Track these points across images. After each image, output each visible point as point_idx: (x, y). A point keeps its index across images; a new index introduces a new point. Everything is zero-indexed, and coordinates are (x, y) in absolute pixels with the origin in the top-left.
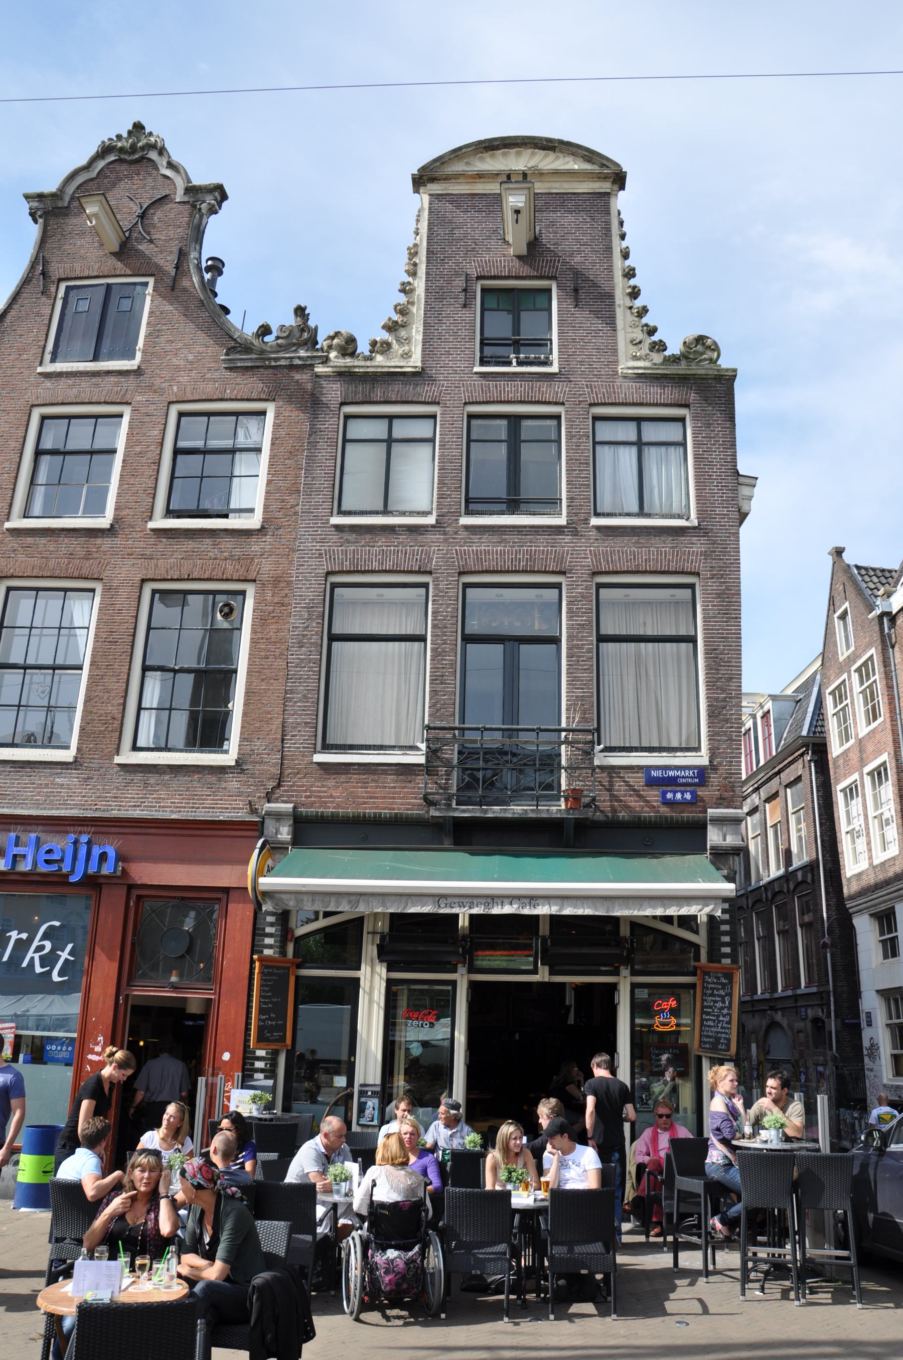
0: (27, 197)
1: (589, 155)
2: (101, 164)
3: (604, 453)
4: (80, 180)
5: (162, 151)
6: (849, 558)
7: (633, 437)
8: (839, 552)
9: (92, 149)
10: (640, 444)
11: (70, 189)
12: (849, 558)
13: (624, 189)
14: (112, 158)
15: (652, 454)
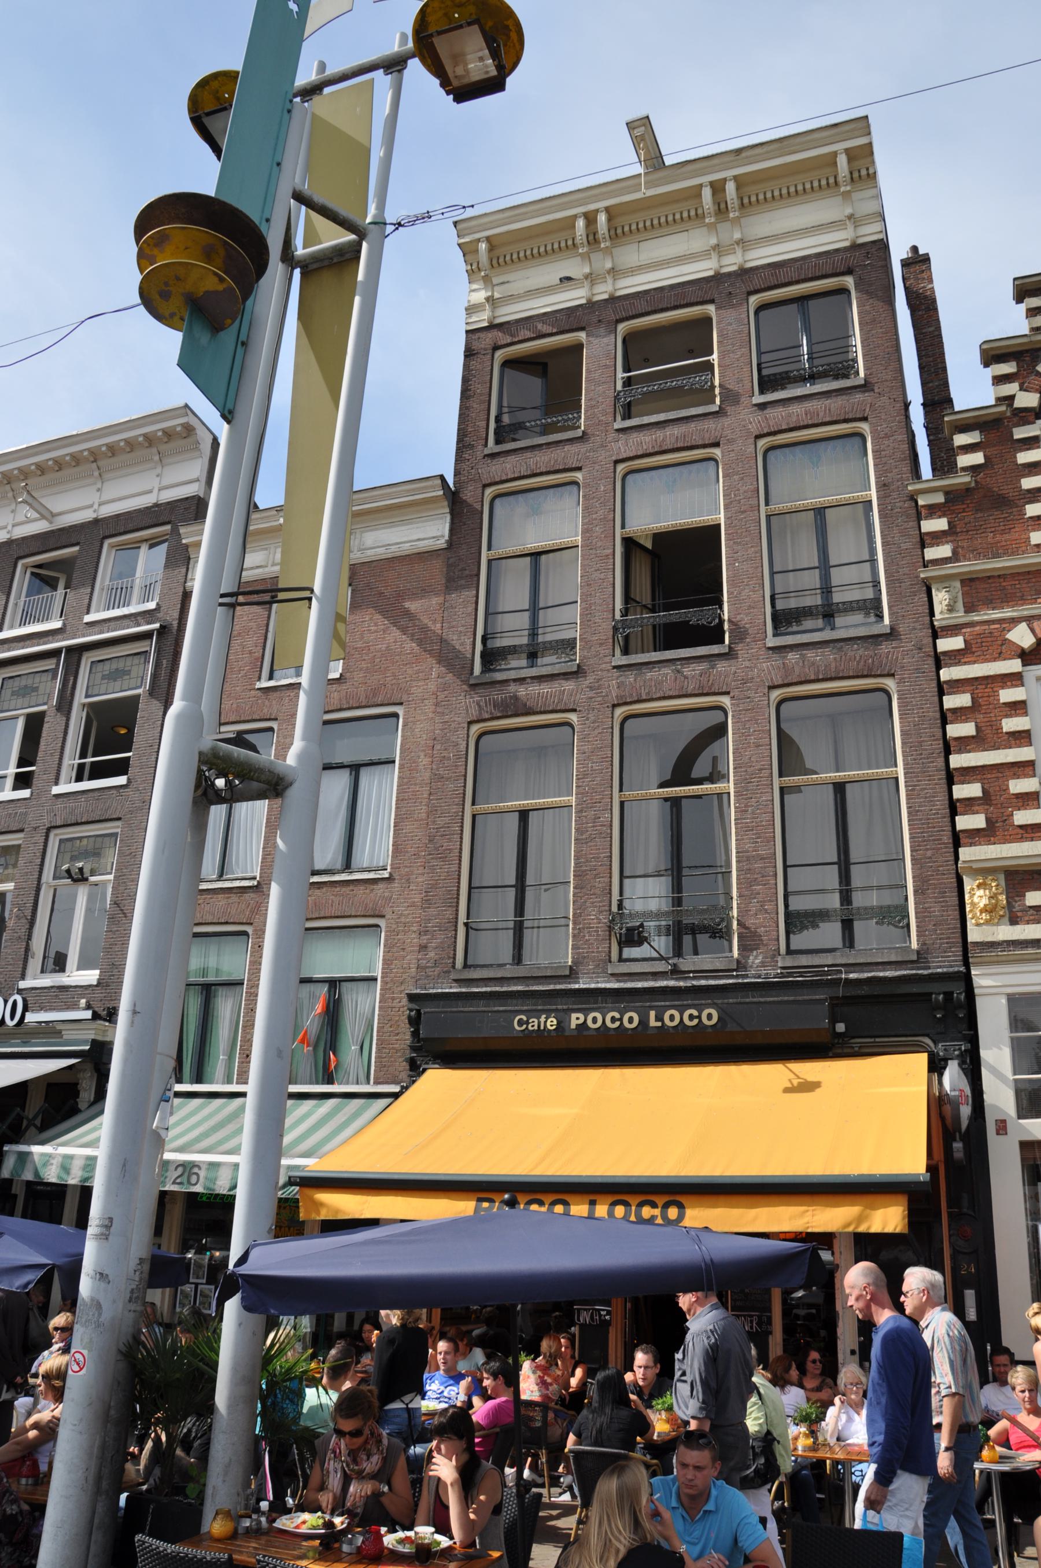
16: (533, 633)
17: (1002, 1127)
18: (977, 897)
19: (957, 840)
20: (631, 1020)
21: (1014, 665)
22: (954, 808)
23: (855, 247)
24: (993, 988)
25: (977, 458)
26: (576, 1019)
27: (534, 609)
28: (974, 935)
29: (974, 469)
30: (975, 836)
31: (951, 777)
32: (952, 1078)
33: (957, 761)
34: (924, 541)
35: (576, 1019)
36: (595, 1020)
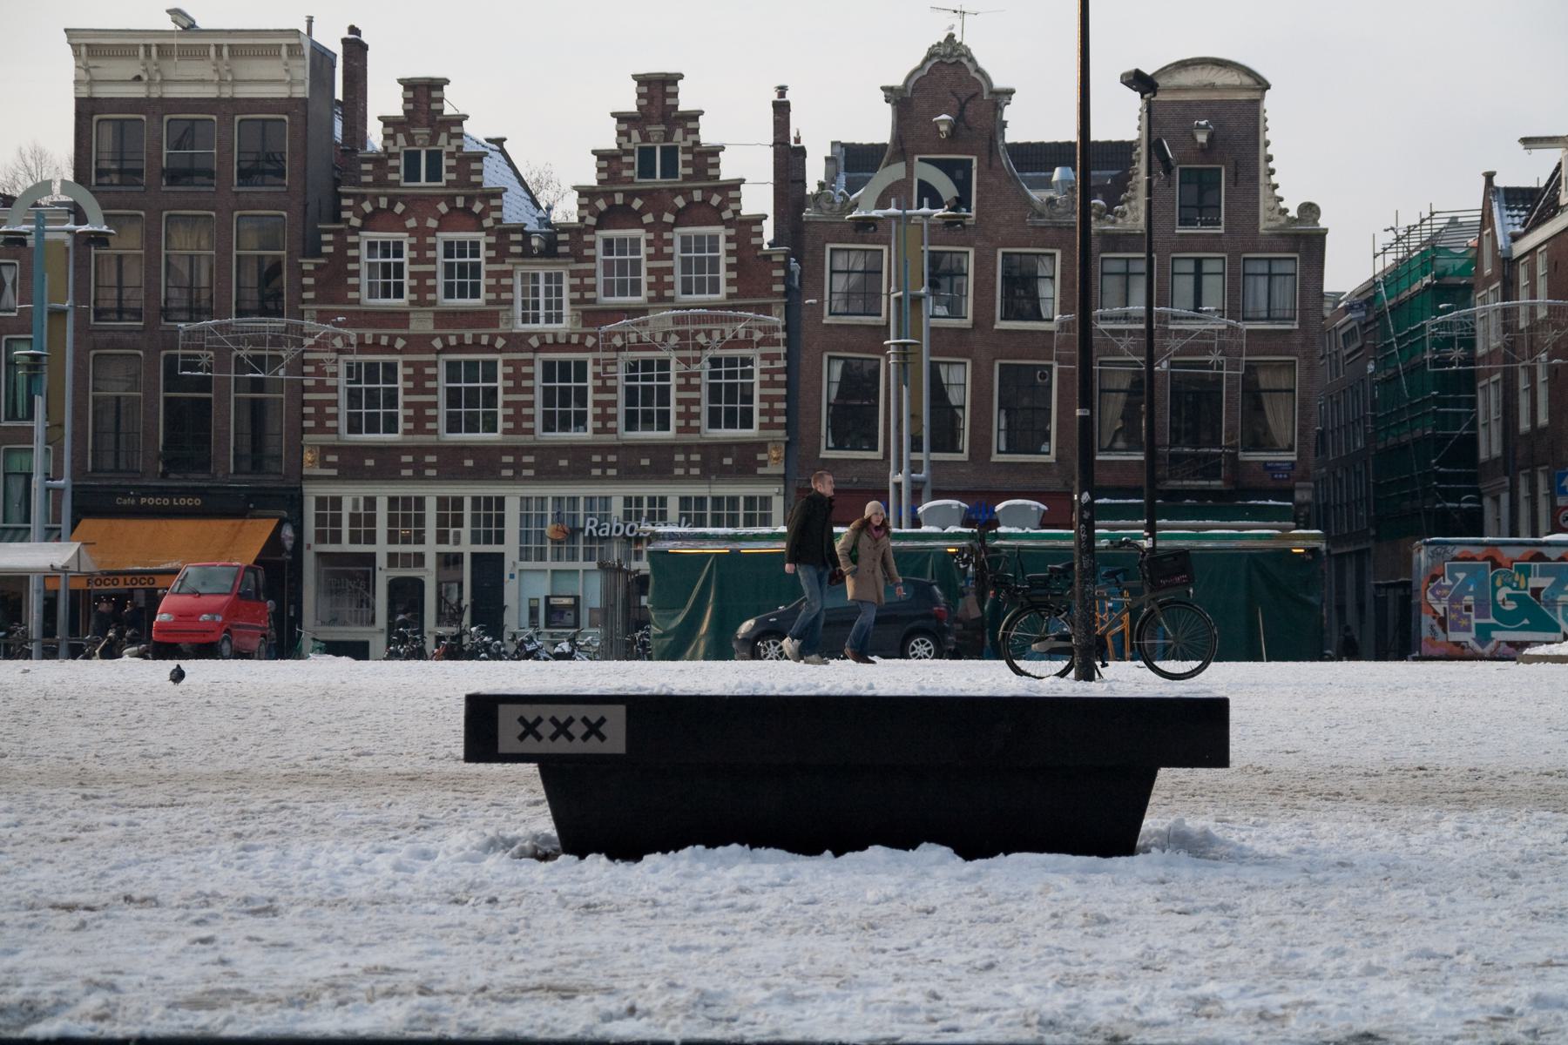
0: (883, 88)
1: (1249, 72)
2: (929, 65)
3: (1251, 280)
4: (917, 77)
5: (972, 60)
6: (1499, 182)
7: (1266, 270)
8: (1489, 177)
9: (924, 54)
10: (1270, 275)
11: (911, 84)
12: (1499, 182)
13: (1268, 87)
14: (936, 60)
15: (1277, 281)
16: (120, 300)
17: (309, 547)
18: (308, 457)
19: (304, 430)
20: (166, 502)
21: (333, 356)
22: (304, 417)
23: (290, 99)
24: (312, 493)
25: (330, 249)
26: (143, 500)
27: (120, 287)
28: (305, 472)
29: (328, 255)
30: (310, 431)
31: (304, 403)
32: (288, 532)
33: (307, 396)
34: (305, 288)
35: (143, 500)
36: (151, 501)
